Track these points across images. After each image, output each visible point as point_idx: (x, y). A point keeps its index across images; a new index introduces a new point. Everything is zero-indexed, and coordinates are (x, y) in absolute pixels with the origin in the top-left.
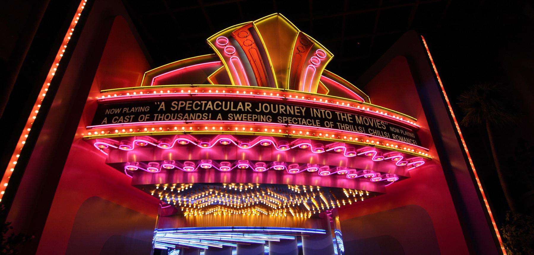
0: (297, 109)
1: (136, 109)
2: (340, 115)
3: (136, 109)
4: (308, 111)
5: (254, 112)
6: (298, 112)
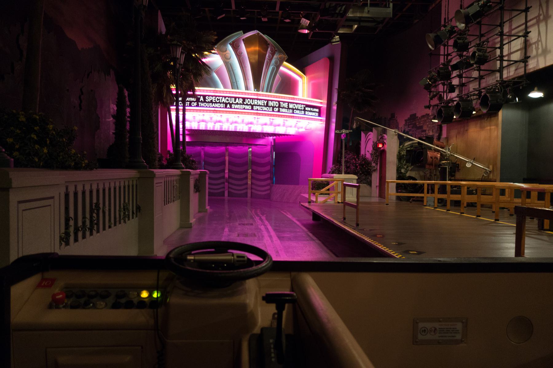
0: (263, 102)
1: (189, 99)
2: (282, 104)
3: (189, 99)
4: (267, 103)
5: (243, 104)
6: (263, 104)
